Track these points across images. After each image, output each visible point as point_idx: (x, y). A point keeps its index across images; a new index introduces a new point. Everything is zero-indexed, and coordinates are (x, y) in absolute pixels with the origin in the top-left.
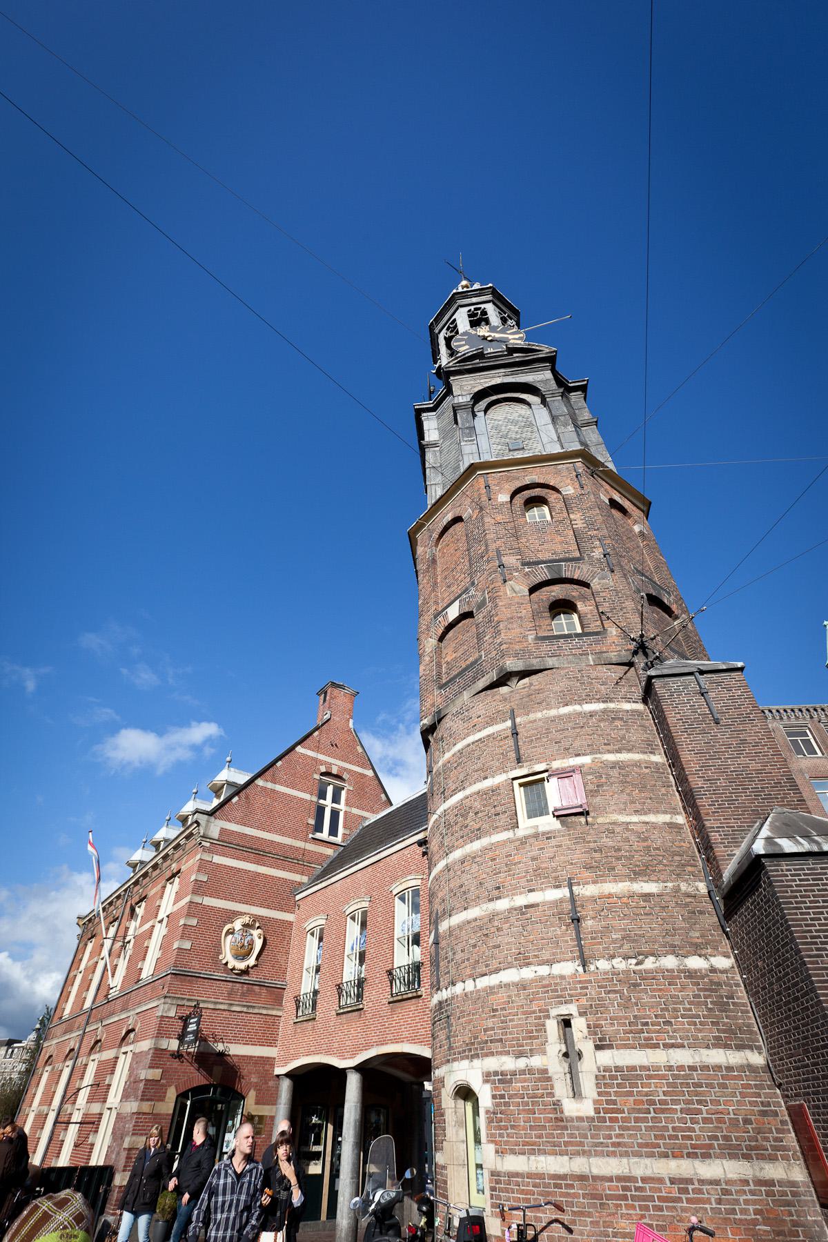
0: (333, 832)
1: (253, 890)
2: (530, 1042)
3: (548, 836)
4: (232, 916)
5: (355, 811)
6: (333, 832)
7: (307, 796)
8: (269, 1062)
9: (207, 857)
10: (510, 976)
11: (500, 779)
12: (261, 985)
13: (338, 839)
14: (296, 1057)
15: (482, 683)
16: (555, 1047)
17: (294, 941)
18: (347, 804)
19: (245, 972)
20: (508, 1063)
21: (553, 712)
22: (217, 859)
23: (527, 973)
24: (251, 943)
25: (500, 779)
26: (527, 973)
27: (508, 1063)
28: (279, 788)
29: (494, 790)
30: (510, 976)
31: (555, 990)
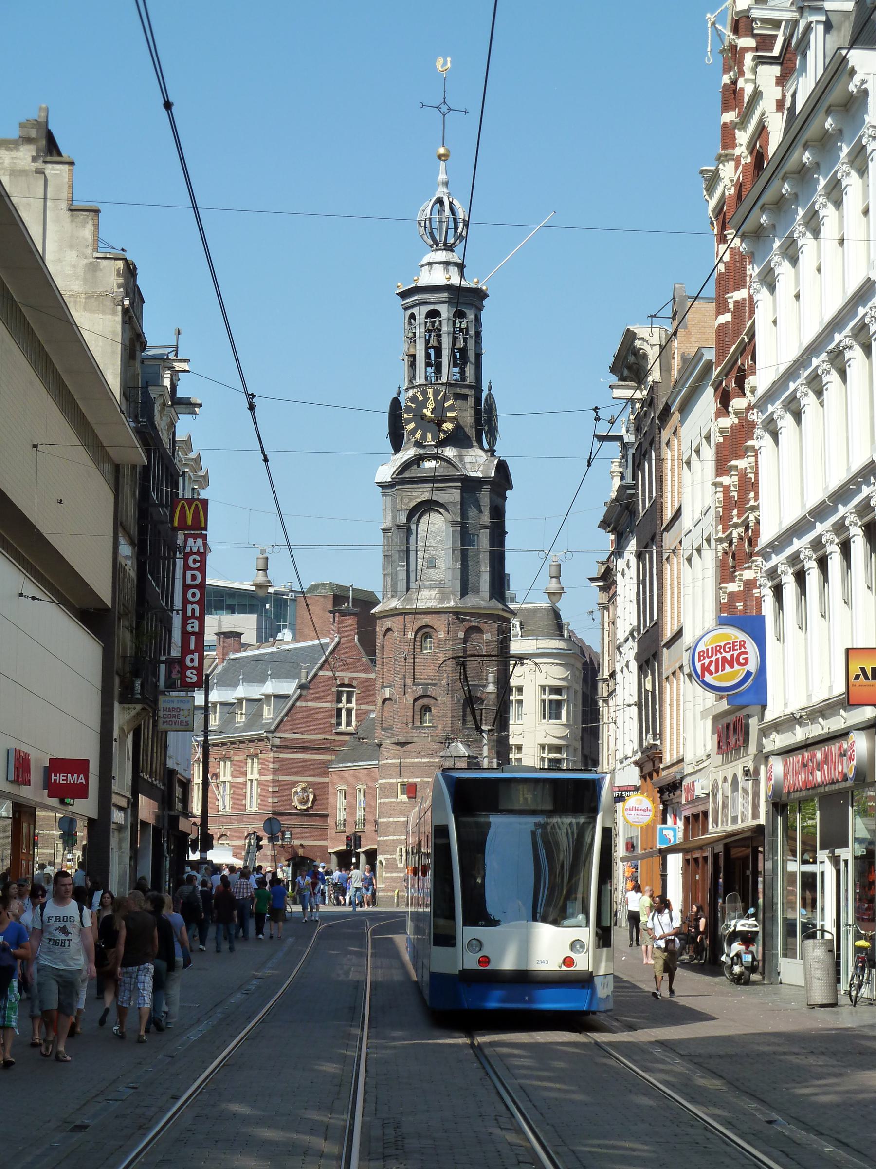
0: (349, 724)
1: (305, 768)
2: (394, 852)
3: (405, 803)
4: (294, 784)
5: (363, 707)
6: (349, 724)
7: (328, 705)
8: (326, 847)
9: (276, 755)
10: (391, 838)
11: (394, 781)
12: (315, 815)
13: (351, 729)
14: (338, 846)
15: (394, 740)
16: (398, 853)
17: (331, 793)
18: (357, 704)
19: (305, 810)
20: (389, 857)
21: (412, 760)
22: (282, 755)
23: (395, 838)
24: (308, 796)
25: (394, 781)
26: (395, 838)
27: (389, 857)
28: (310, 704)
29: (393, 784)
30: (391, 838)
31: (399, 841)
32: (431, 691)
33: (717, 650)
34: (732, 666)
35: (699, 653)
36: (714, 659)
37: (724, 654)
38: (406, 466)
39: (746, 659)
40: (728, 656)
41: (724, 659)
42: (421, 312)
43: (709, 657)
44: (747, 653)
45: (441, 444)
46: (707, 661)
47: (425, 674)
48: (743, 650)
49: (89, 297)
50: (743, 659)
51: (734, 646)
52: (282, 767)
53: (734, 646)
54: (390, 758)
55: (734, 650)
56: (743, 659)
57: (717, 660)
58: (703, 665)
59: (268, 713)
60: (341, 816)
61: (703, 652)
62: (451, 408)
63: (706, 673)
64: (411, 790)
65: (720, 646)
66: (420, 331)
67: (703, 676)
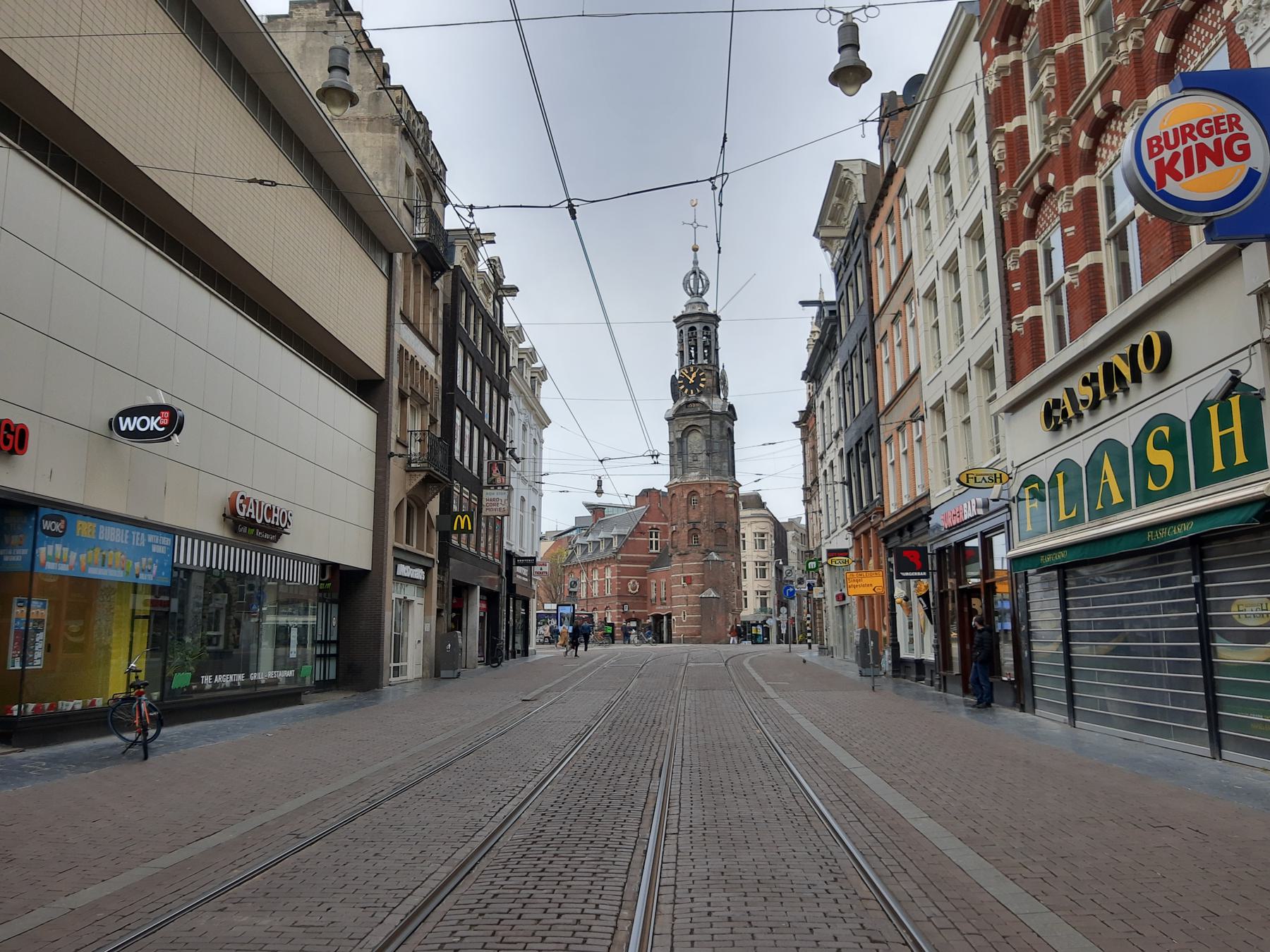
32: (699, 526)
33: (1185, 132)
34: (1219, 162)
35: (1149, 141)
36: (1180, 149)
37: (1200, 140)
38: (680, 407)
39: (1246, 150)
40: (1209, 142)
41: (1202, 148)
42: (685, 329)
43: (1170, 147)
44: (1245, 137)
45: (699, 394)
46: (1167, 155)
47: (694, 516)
48: (1236, 131)
49: (371, 120)
50: (1240, 147)
51: (1218, 125)
52: (622, 572)
53: (1218, 125)
54: (676, 563)
55: (1219, 132)
56: (1240, 147)
57: (1188, 151)
58: (1159, 164)
59: (615, 545)
60: (653, 595)
61: (1158, 138)
62: (703, 376)
63: (1168, 177)
64: (688, 580)
65: (1190, 126)
66: (685, 338)
67: (1162, 182)
